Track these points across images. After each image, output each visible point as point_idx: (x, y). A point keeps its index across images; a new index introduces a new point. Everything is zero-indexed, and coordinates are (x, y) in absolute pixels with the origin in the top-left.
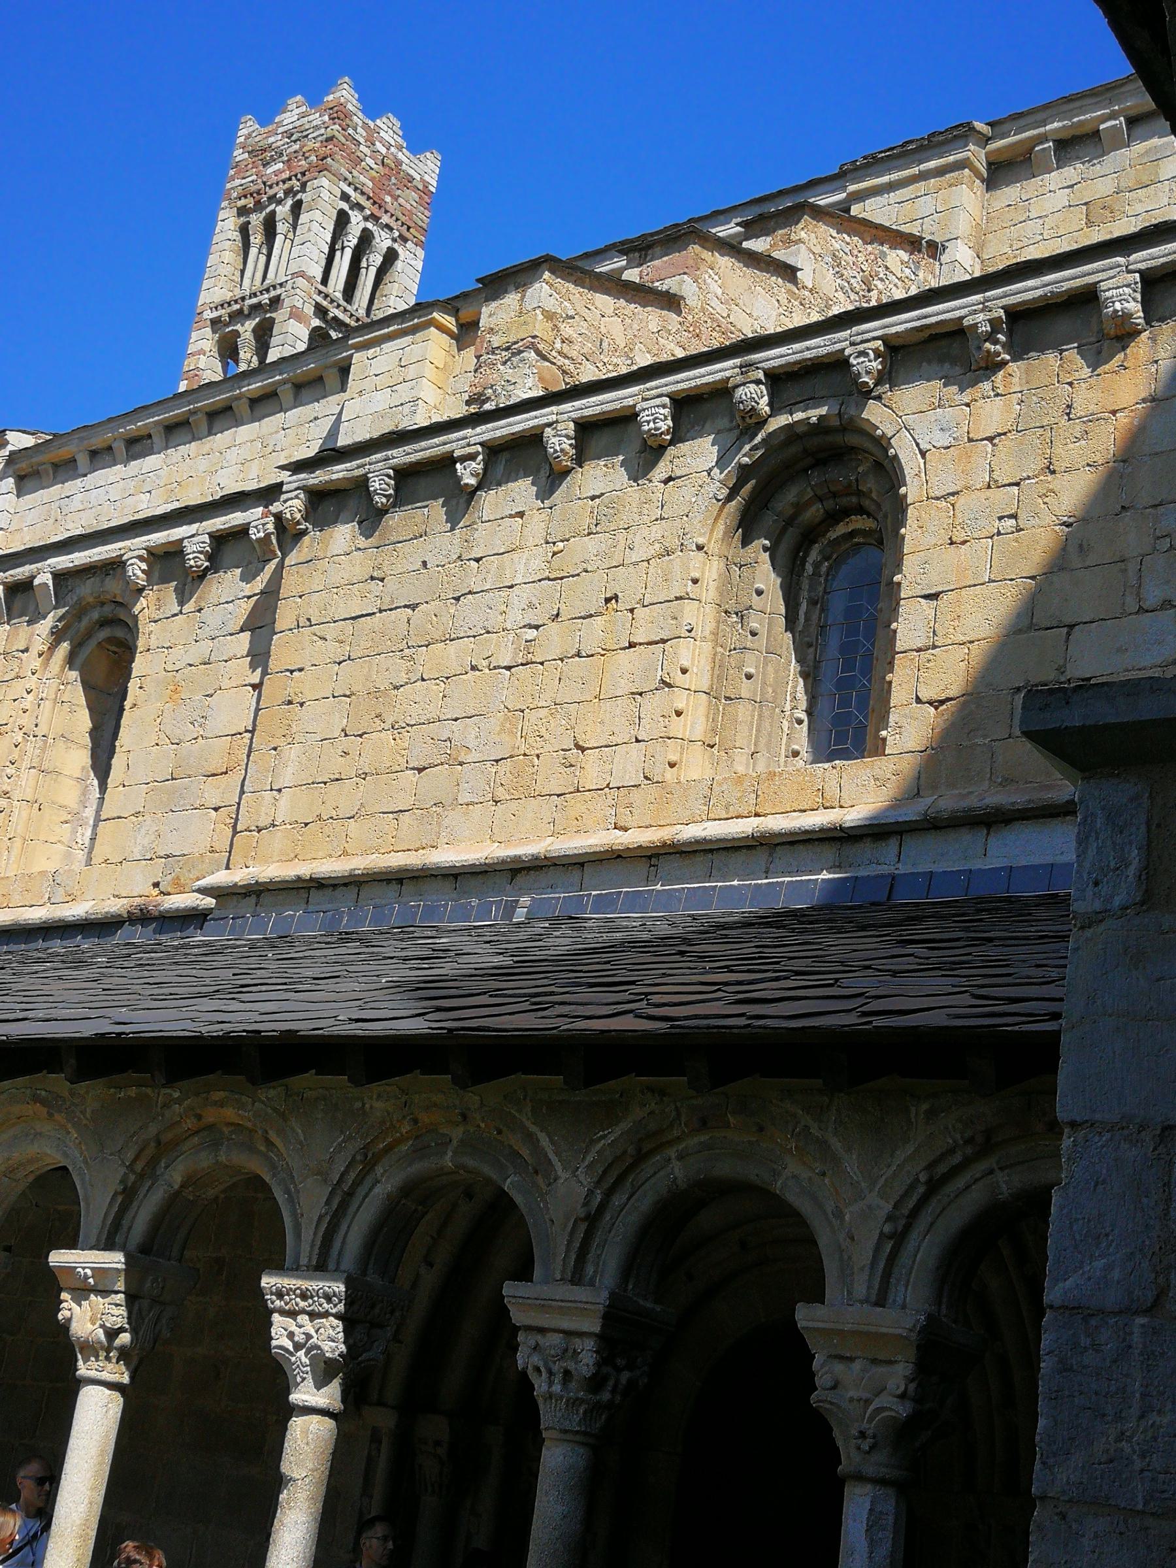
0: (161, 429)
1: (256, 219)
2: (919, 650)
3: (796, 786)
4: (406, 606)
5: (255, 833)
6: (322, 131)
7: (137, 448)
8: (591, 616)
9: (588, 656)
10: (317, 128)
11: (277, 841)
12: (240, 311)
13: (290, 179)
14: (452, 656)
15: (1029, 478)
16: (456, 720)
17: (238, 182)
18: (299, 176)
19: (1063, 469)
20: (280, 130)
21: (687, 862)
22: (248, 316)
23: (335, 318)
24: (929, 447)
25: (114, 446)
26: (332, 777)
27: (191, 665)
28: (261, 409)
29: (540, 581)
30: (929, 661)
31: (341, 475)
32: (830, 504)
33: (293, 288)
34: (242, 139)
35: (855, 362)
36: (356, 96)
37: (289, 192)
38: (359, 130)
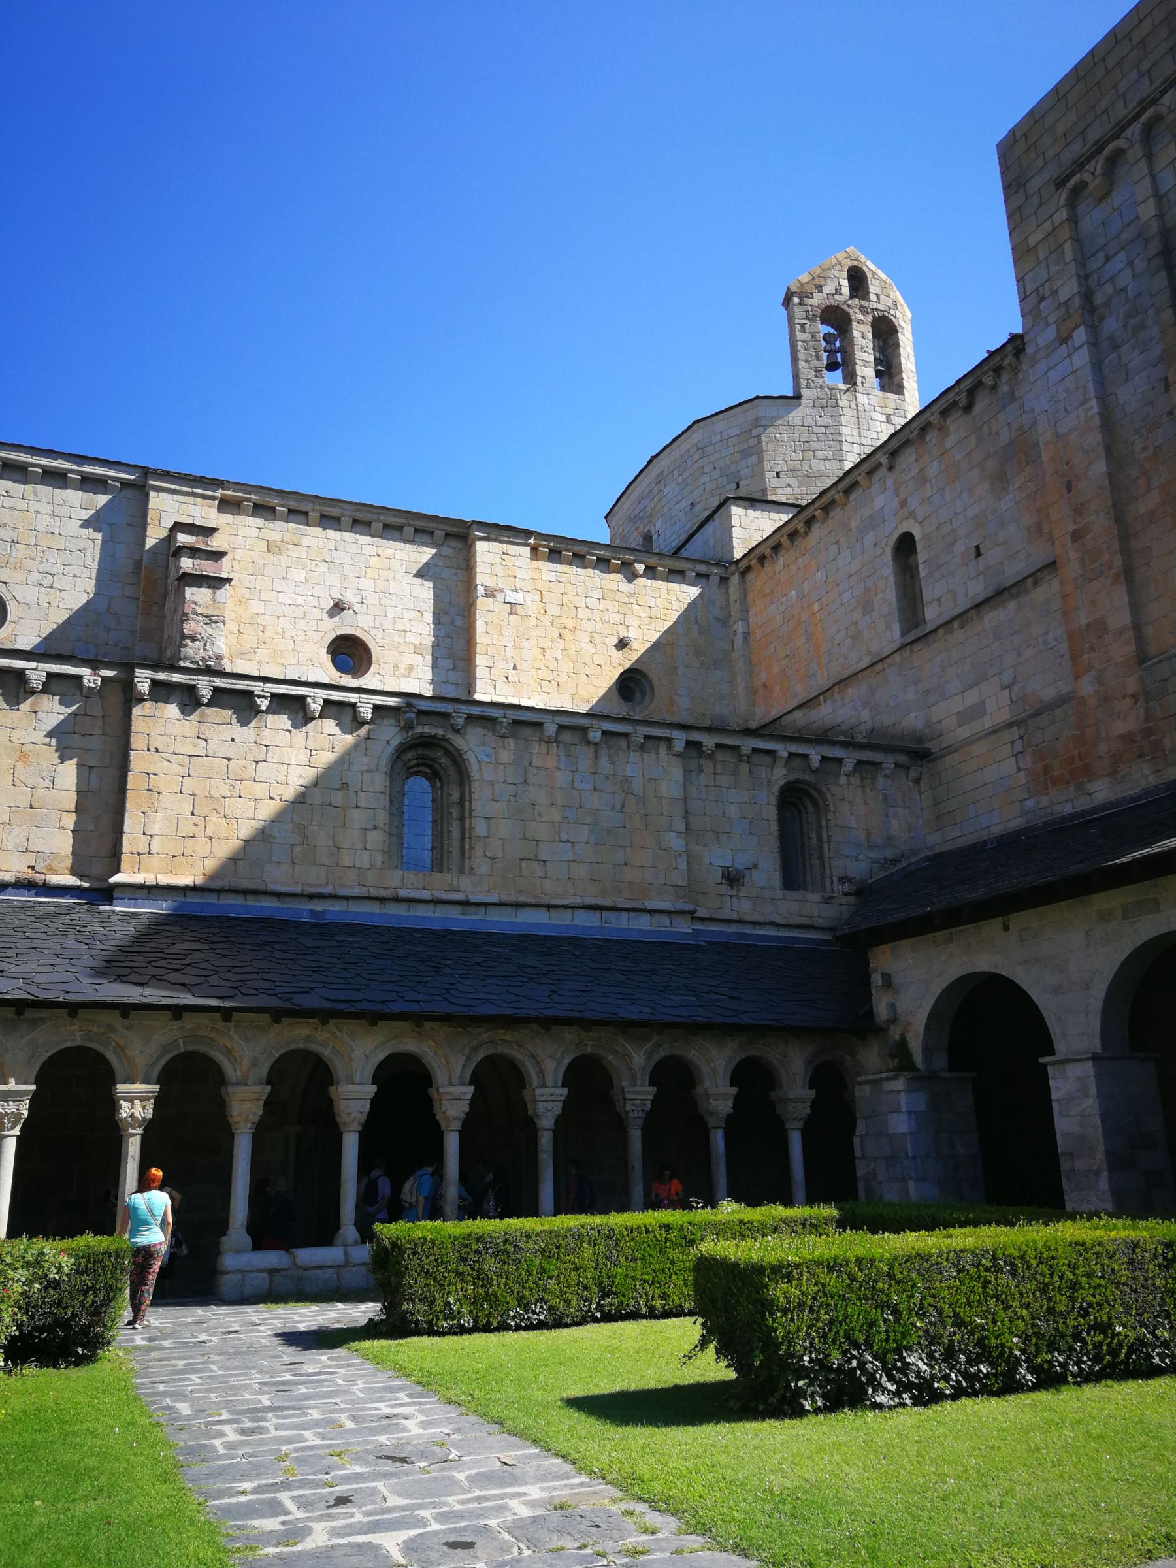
11: (155, 861)
31: (179, 680)
32: (420, 761)
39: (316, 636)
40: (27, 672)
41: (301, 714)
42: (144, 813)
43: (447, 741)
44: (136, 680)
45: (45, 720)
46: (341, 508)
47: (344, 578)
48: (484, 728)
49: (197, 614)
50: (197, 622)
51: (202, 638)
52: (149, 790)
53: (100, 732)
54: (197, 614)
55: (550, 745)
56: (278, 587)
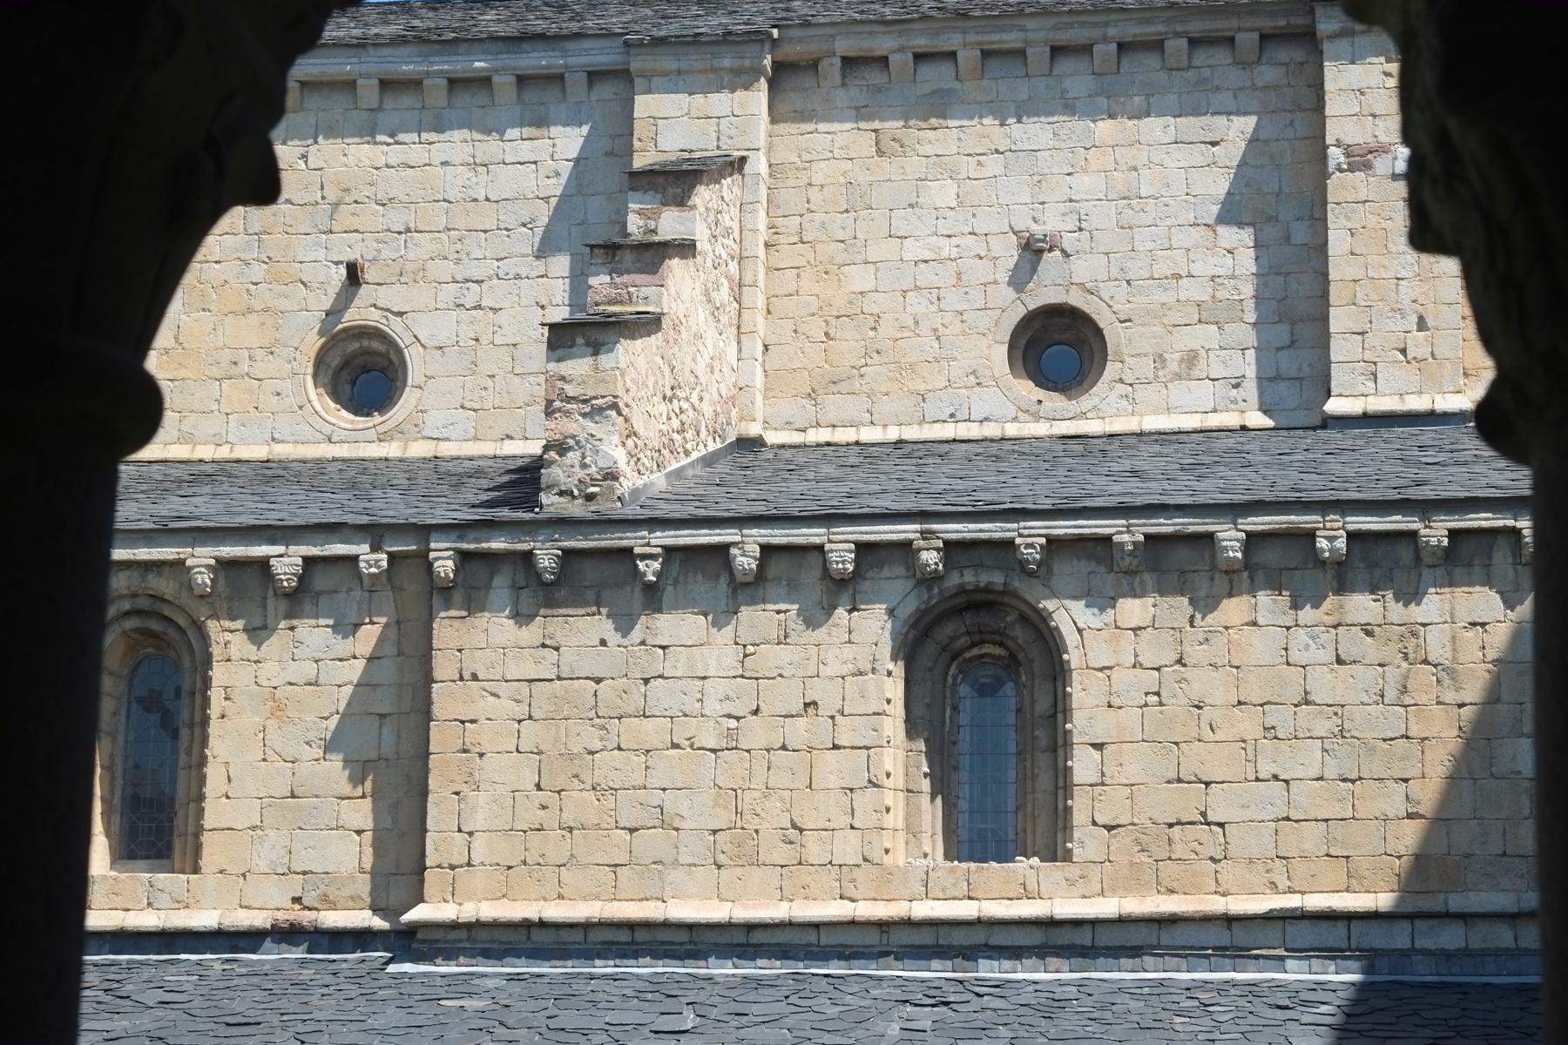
2: (1091, 785)
3: (1002, 880)
4: (588, 678)
5: (448, 870)
8: (792, 716)
9: (794, 751)
11: (478, 879)
14: (652, 731)
15: (1166, 666)
16: (664, 790)
19: (1192, 664)
21: (916, 931)
24: (1085, 627)
26: (532, 827)
27: (291, 684)
29: (735, 677)
30: (1100, 795)
32: (976, 638)
35: (1025, 552)
39: (985, 321)
40: (273, 561)
41: (723, 581)
42: (457, 793)
43: (1015, 594)
44: (432, 555)
45: (308, 641)
46: (1022, 29)
47: (1039, 179)
48: (1090, 557)
49: (569, 399)
50: (567, 414)
51: (578, 443)
52: (465, 751)
53: (395, 651)
54: (569, 399)
55: (1235, 577)
56: (900, 227)
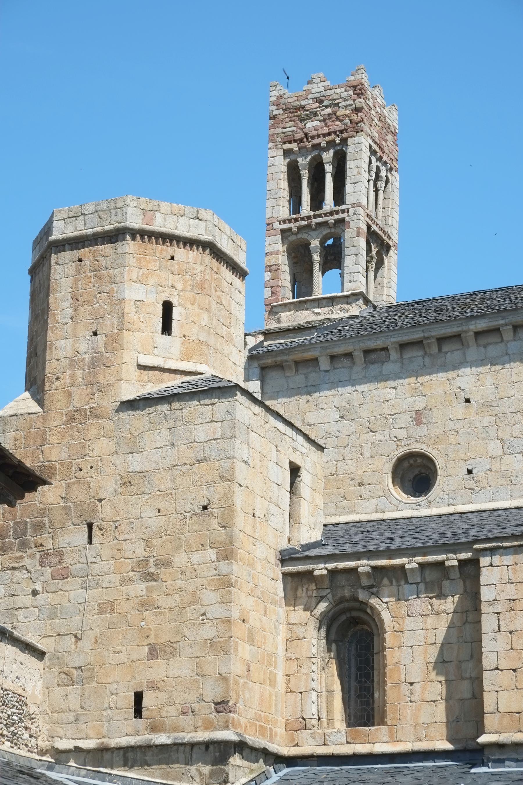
0: (397, 346)
1: (303, 161)
6: (351, 102)
7: (373, 356)
10: (345, 99)
12: (308, 227)
13: (329, 134)
17: (280, 130)
18: (338, 133)
20: (310, 96)
22: (314, 230)
23: (374, 231)
25: (355, 354)
28: (483, 341)
33: (355, 214)
34: (274, 99)
36: (367, 77)
37: (331, 144)
38: (371, 100)
